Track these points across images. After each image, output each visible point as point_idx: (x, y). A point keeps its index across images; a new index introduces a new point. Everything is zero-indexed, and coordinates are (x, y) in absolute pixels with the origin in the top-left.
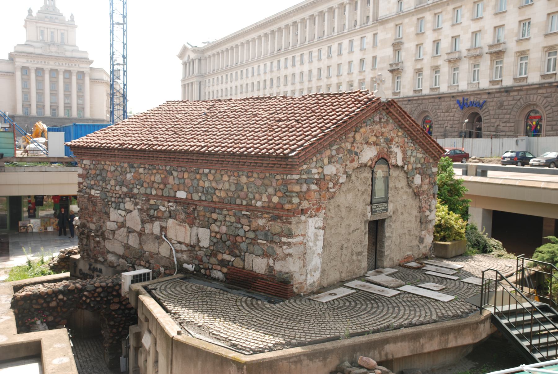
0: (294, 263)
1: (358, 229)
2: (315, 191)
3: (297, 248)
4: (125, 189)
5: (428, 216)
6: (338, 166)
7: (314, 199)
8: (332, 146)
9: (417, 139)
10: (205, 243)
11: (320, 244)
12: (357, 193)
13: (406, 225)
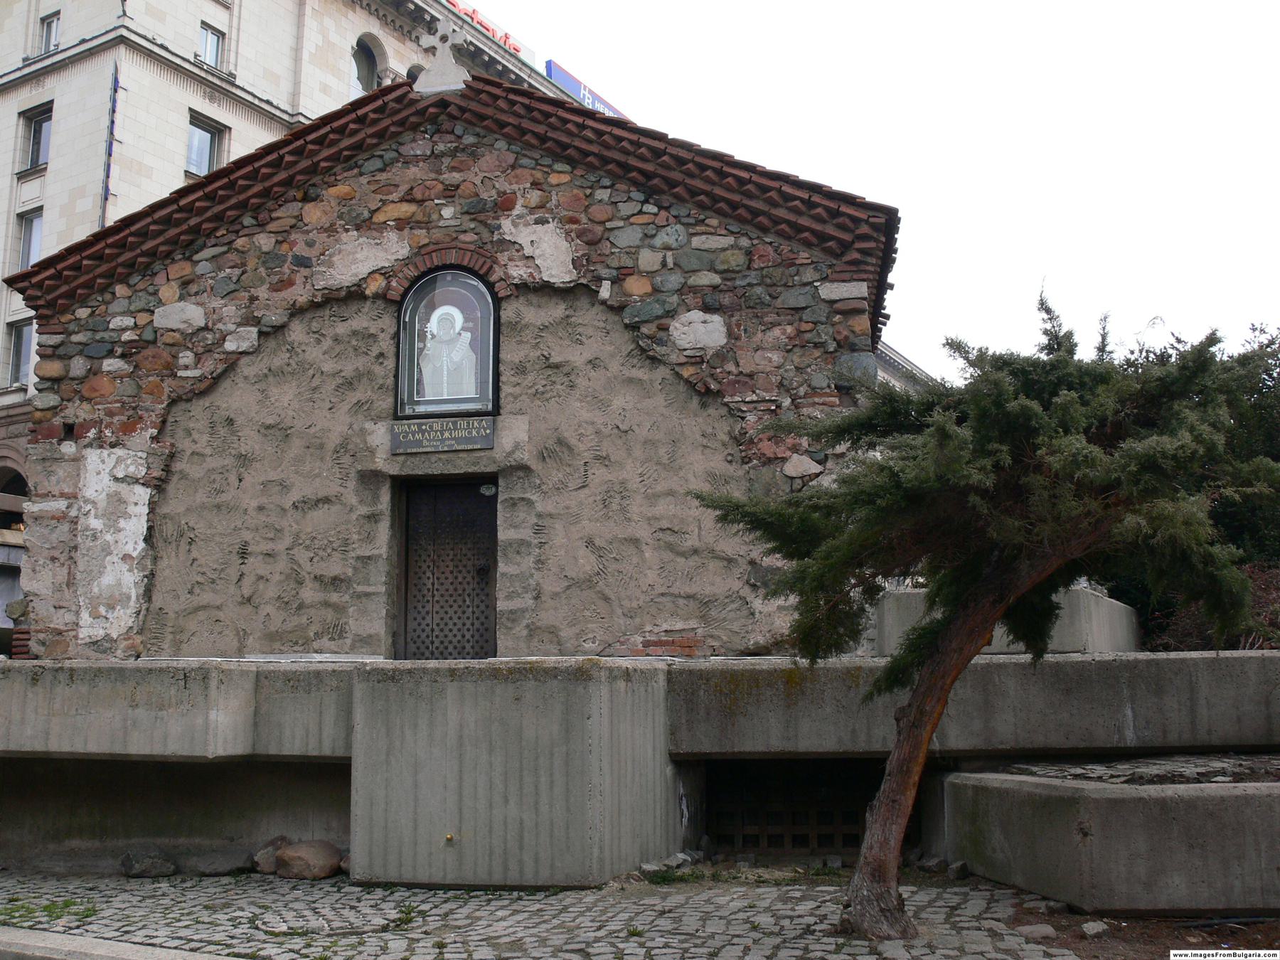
0: (34, 571)
1: (327, 500)
2: (115, 376)
3: (46, 531)
5: (806, 479)
6: (217, 303)
7: (109, 400)
8: (197, 252)
9: (672, 184)
11: (134, 527)
12: (316, 382)
13: (637, 507)
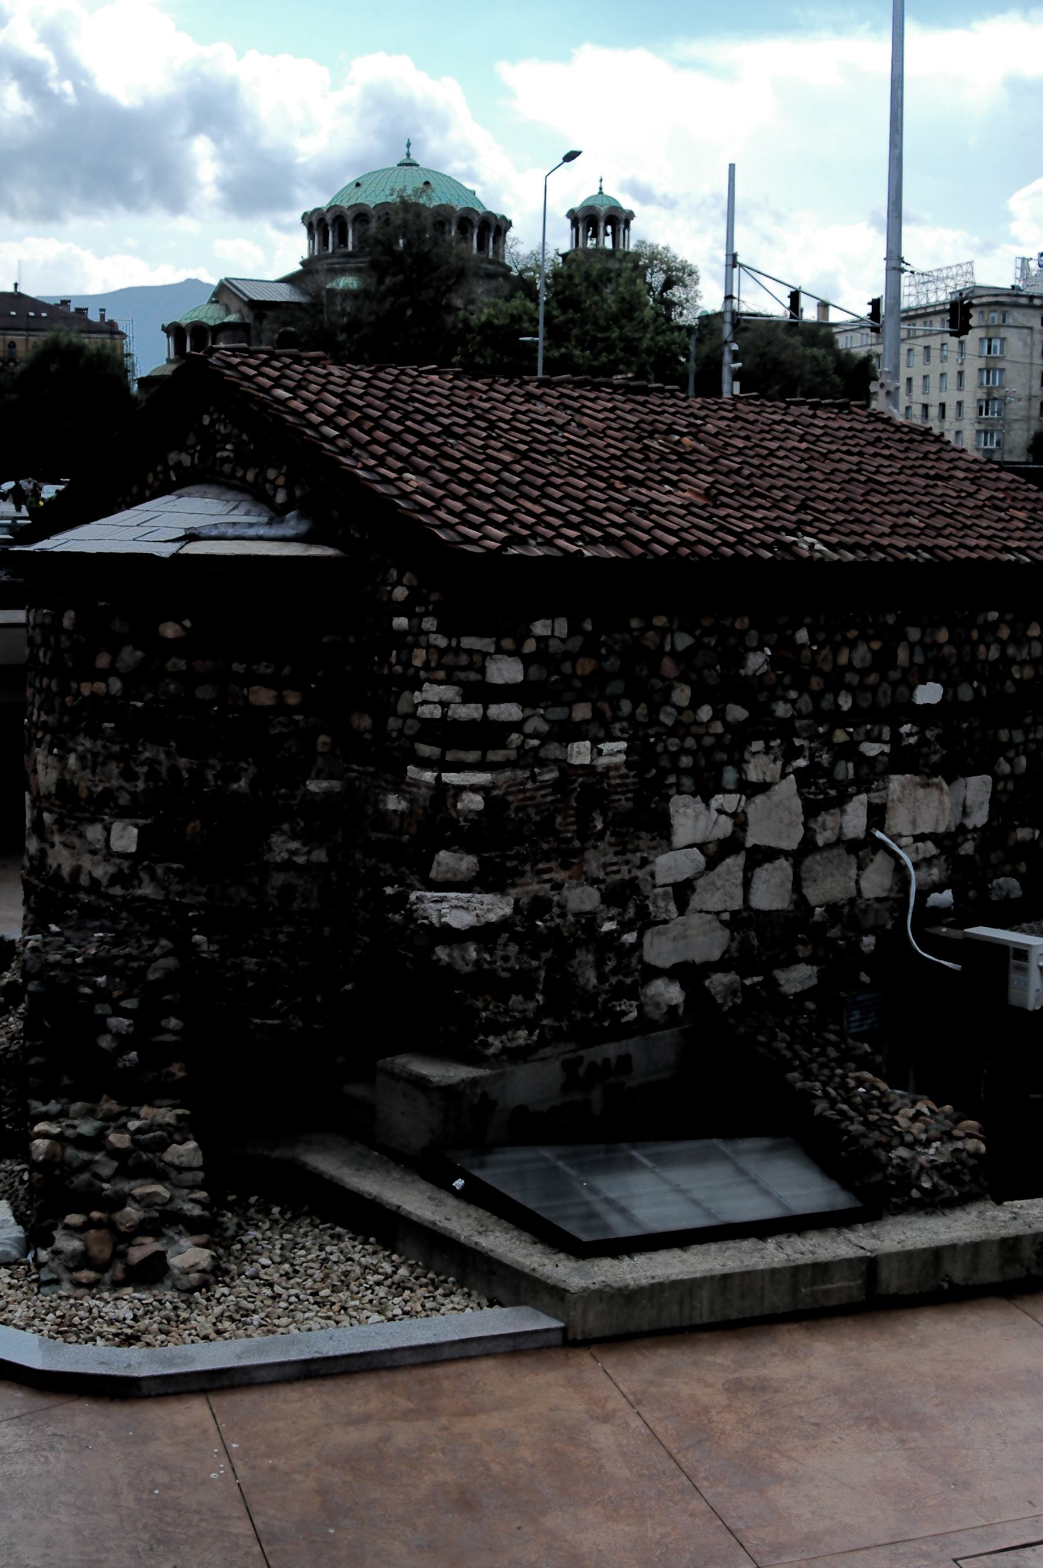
4: (737, 713)
10: (979, 818)
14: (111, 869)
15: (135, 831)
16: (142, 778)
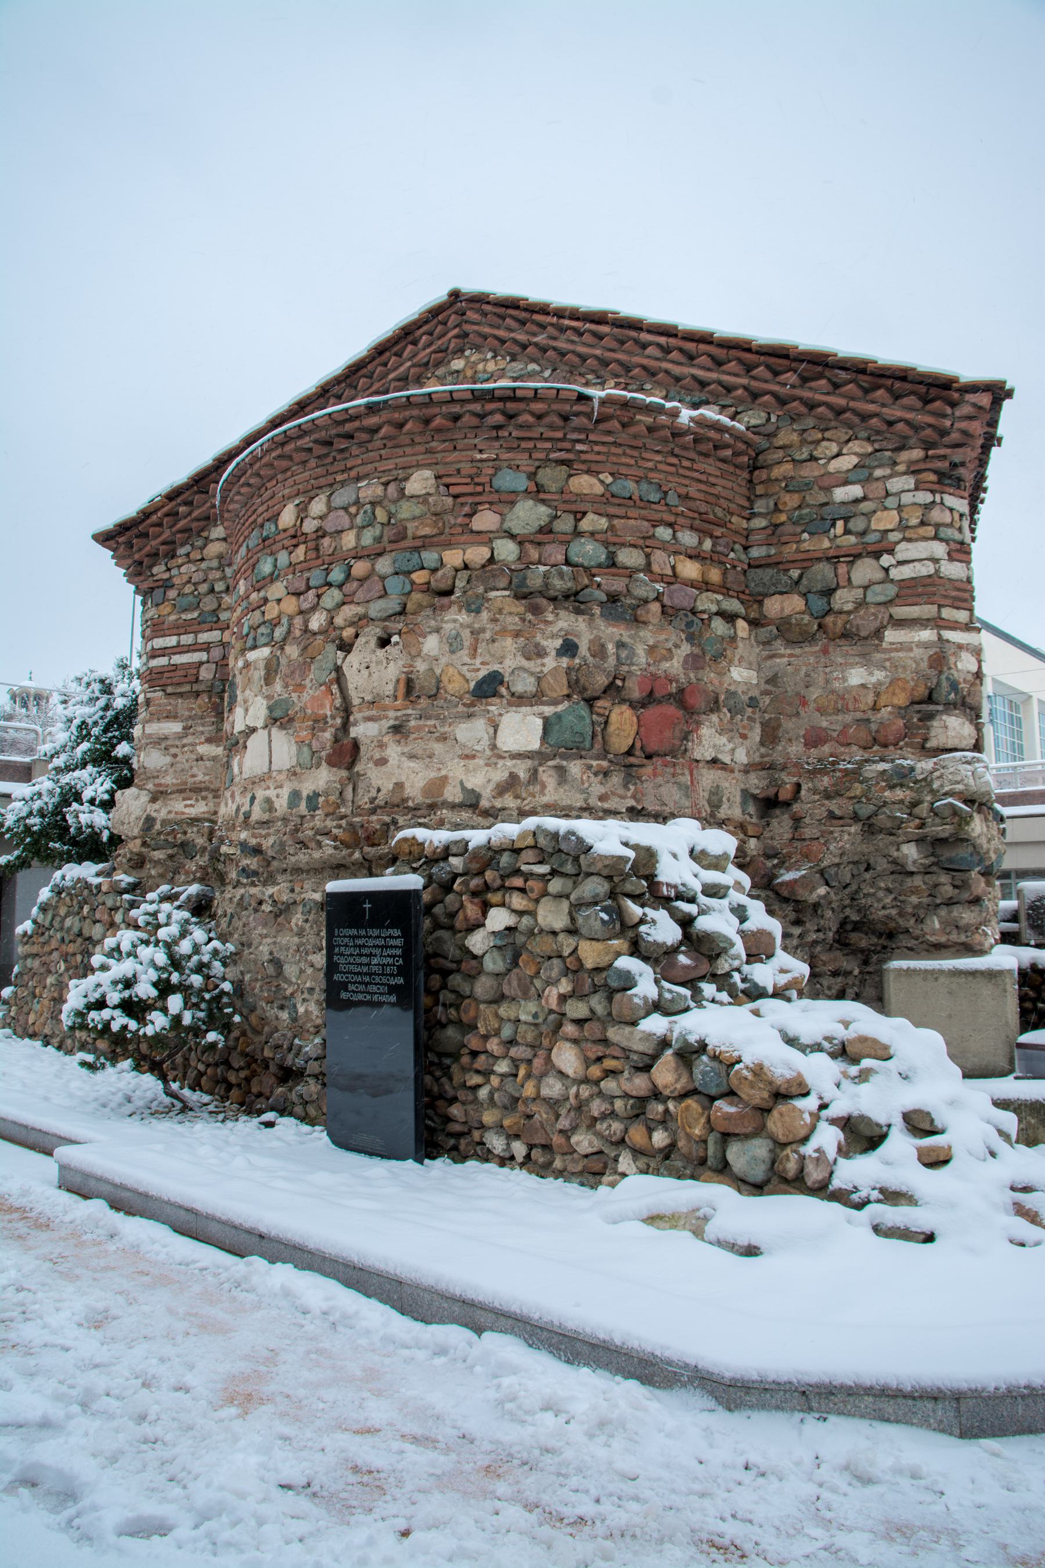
14: (500, 775)
15: (539, 722)
16: (554, 653)
